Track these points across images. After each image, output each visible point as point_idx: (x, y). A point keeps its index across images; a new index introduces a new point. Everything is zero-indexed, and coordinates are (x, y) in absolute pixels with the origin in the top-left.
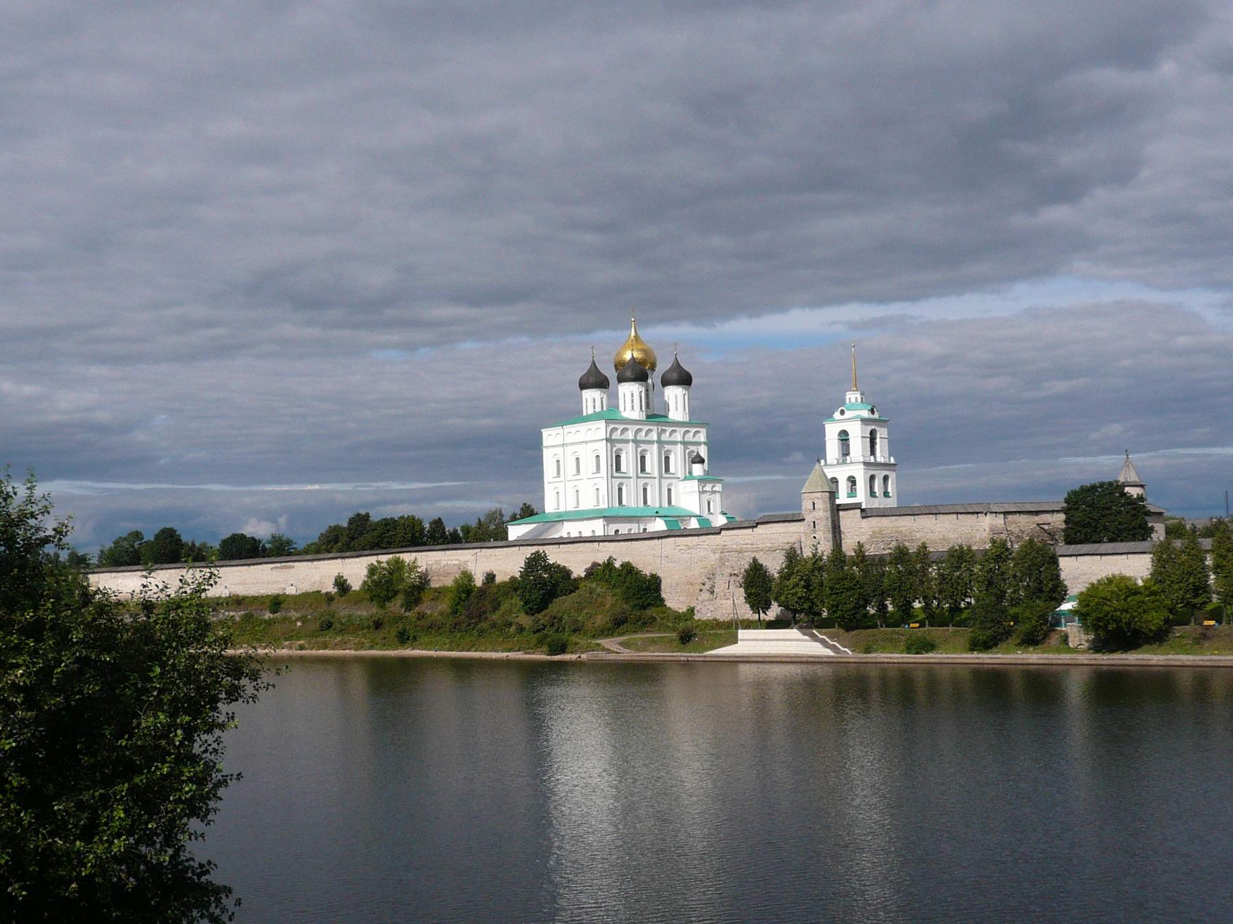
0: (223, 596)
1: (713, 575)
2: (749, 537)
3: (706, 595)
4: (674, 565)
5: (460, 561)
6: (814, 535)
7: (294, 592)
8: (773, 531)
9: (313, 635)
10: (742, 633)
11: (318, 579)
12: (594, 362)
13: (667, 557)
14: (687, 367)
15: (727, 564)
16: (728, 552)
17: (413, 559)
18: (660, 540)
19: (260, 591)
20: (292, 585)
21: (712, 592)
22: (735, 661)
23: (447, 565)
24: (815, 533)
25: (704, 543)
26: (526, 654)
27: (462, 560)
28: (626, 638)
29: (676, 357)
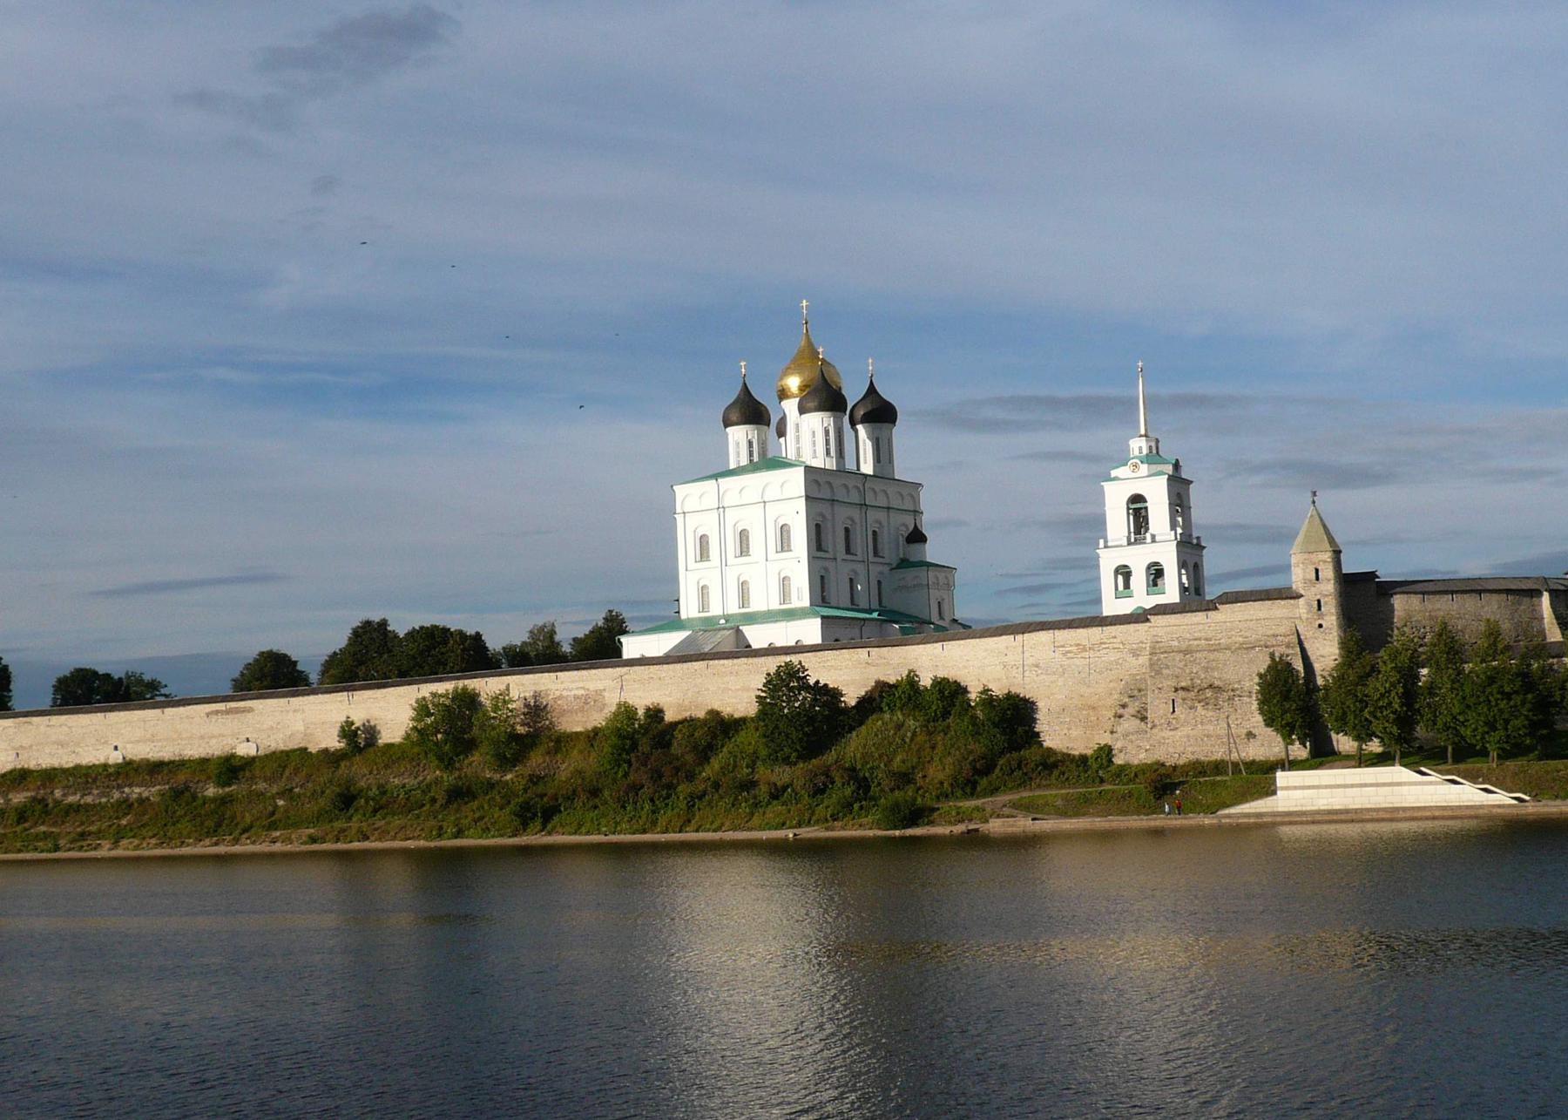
0: (111, 762)
1: (1140, 691)
2: (1201, 627)
3: (1129, 724)
4: (1054, 678)
5: (588, 690)
6: (1320, 622)
7: (253, 752)
8: (1246, 617)
9: (318, 818)
10: (1282, 777)
11: (302, 728)
12: (745, 384)
13: (1037, 666)
14: (886, 392)
15: (1165, 672)
16: (1162, 653)
17: (503, 687)
18: (1019, 637)
19: (185, 752)
20: (248, 740)
21: (1144, 719)
22: (1265, 826)
23: (560, 697)
24: (1323, 619)
25: (1115, 640)
26: (827, 829)
27: (591, 689)
28: (1017, 796)
29: (871, 381)
